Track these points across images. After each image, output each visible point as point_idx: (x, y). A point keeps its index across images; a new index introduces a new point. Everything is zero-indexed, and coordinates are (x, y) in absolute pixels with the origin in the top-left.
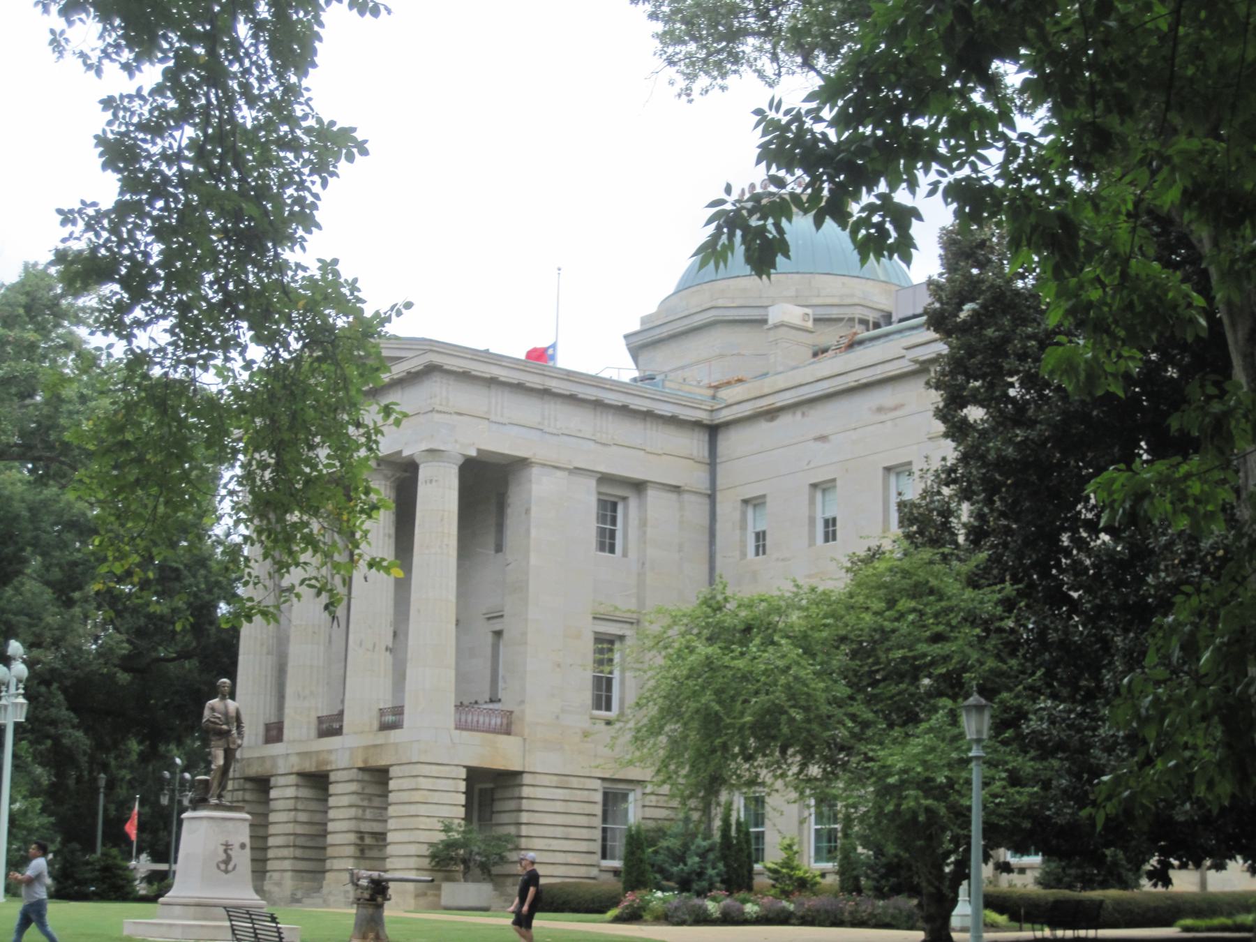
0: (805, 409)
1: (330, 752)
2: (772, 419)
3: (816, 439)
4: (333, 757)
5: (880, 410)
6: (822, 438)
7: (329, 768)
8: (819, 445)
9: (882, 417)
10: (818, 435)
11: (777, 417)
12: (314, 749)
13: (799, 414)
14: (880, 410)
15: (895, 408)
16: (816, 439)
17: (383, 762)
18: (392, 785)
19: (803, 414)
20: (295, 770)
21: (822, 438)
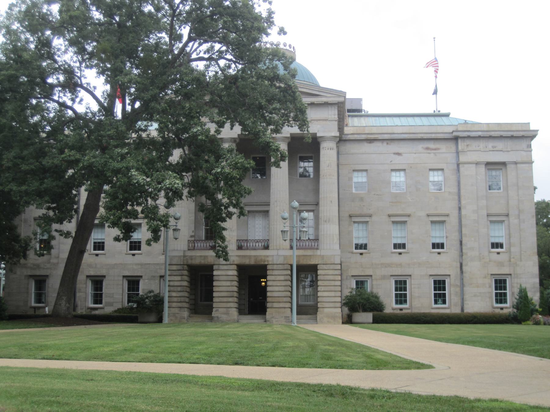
0: (389, 142)
1: (268, 256)
2: (370, 143)
3: (394, 154)
4: (270, 259)
5: (427, 149)
6: (399, 154)
7: (266, 263)
8: (397, 156)
9: (429, 151)
10: (396, 152)
11: (373, 142)
12: (248, 254)
13: (385, 144)
14: (427, 149)
15: (435, 149)
16: (394, 154)
17: (313, 262)
18: (319, 272)
19: (387, 144)
20: (236, 263)
21: (399, 154)
